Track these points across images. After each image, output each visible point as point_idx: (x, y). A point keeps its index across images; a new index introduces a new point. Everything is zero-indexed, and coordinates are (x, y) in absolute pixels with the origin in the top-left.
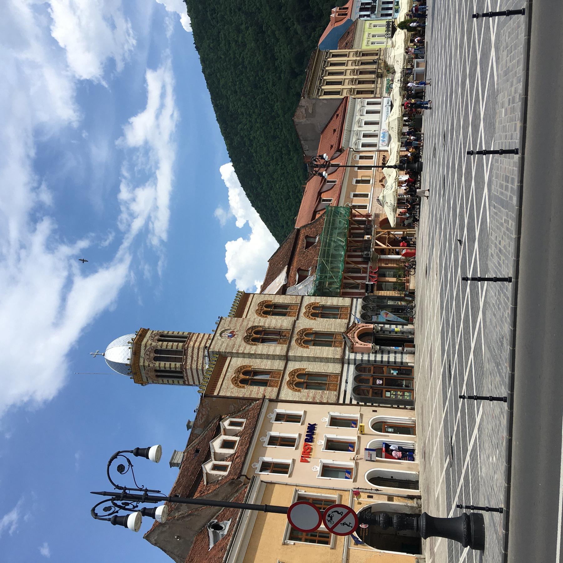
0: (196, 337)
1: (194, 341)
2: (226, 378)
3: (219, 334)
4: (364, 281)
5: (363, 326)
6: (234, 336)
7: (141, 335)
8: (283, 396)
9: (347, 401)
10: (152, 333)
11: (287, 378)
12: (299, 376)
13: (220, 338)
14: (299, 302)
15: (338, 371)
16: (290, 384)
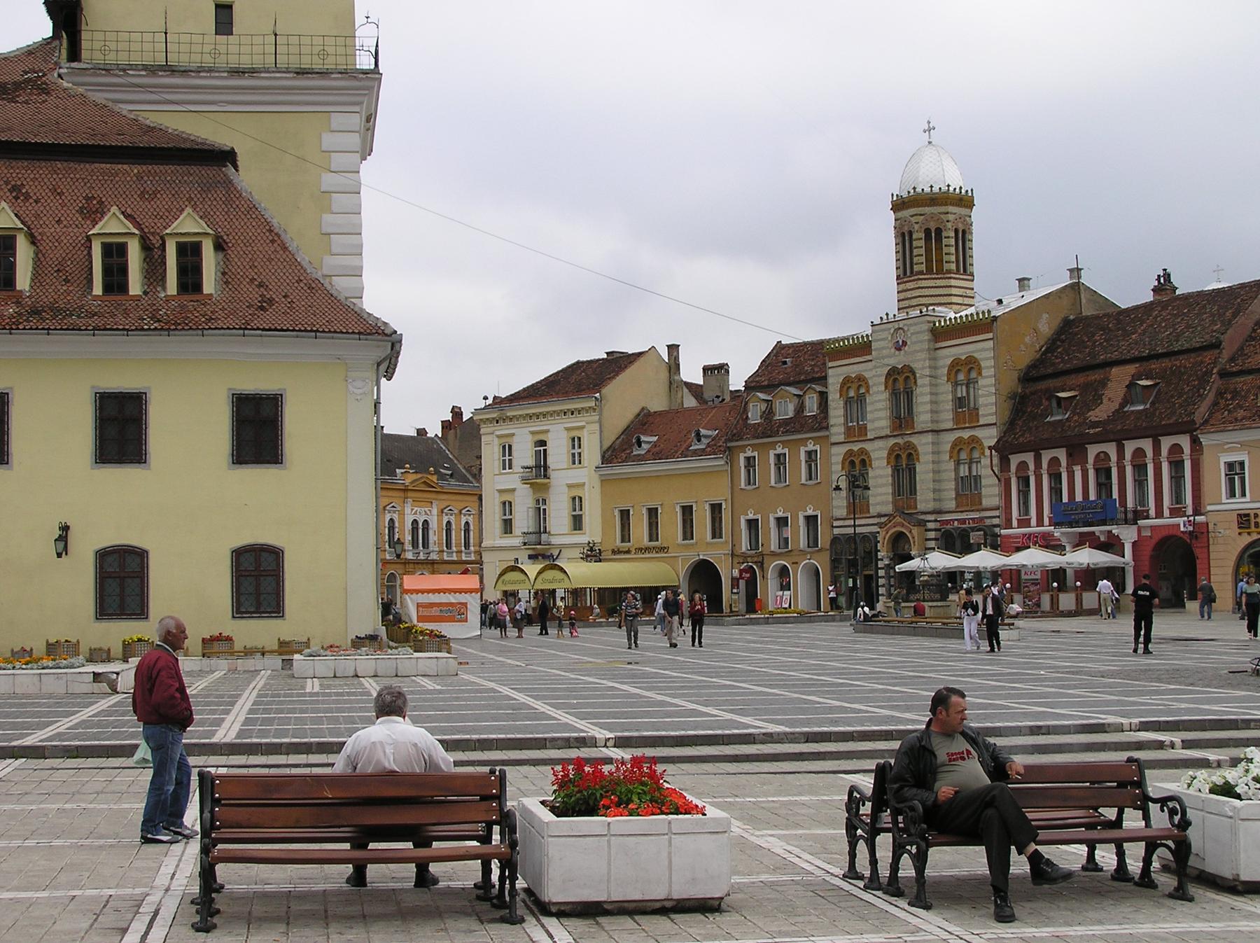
0: (912, 287)
1: (905, 288)
2: (851, 366)
3: (897, 327)
4: (1034, 522)
5: (913, 538)
6: (899, 349)
7: (904, 203)
8: (835, 450)
9: (836, 531)
10: (912, 216)
11: (856, 447)
12: (863, 462)
13: (892, 331)
14: (981, 422)
15: (873, 511)
16: (850, 453)
